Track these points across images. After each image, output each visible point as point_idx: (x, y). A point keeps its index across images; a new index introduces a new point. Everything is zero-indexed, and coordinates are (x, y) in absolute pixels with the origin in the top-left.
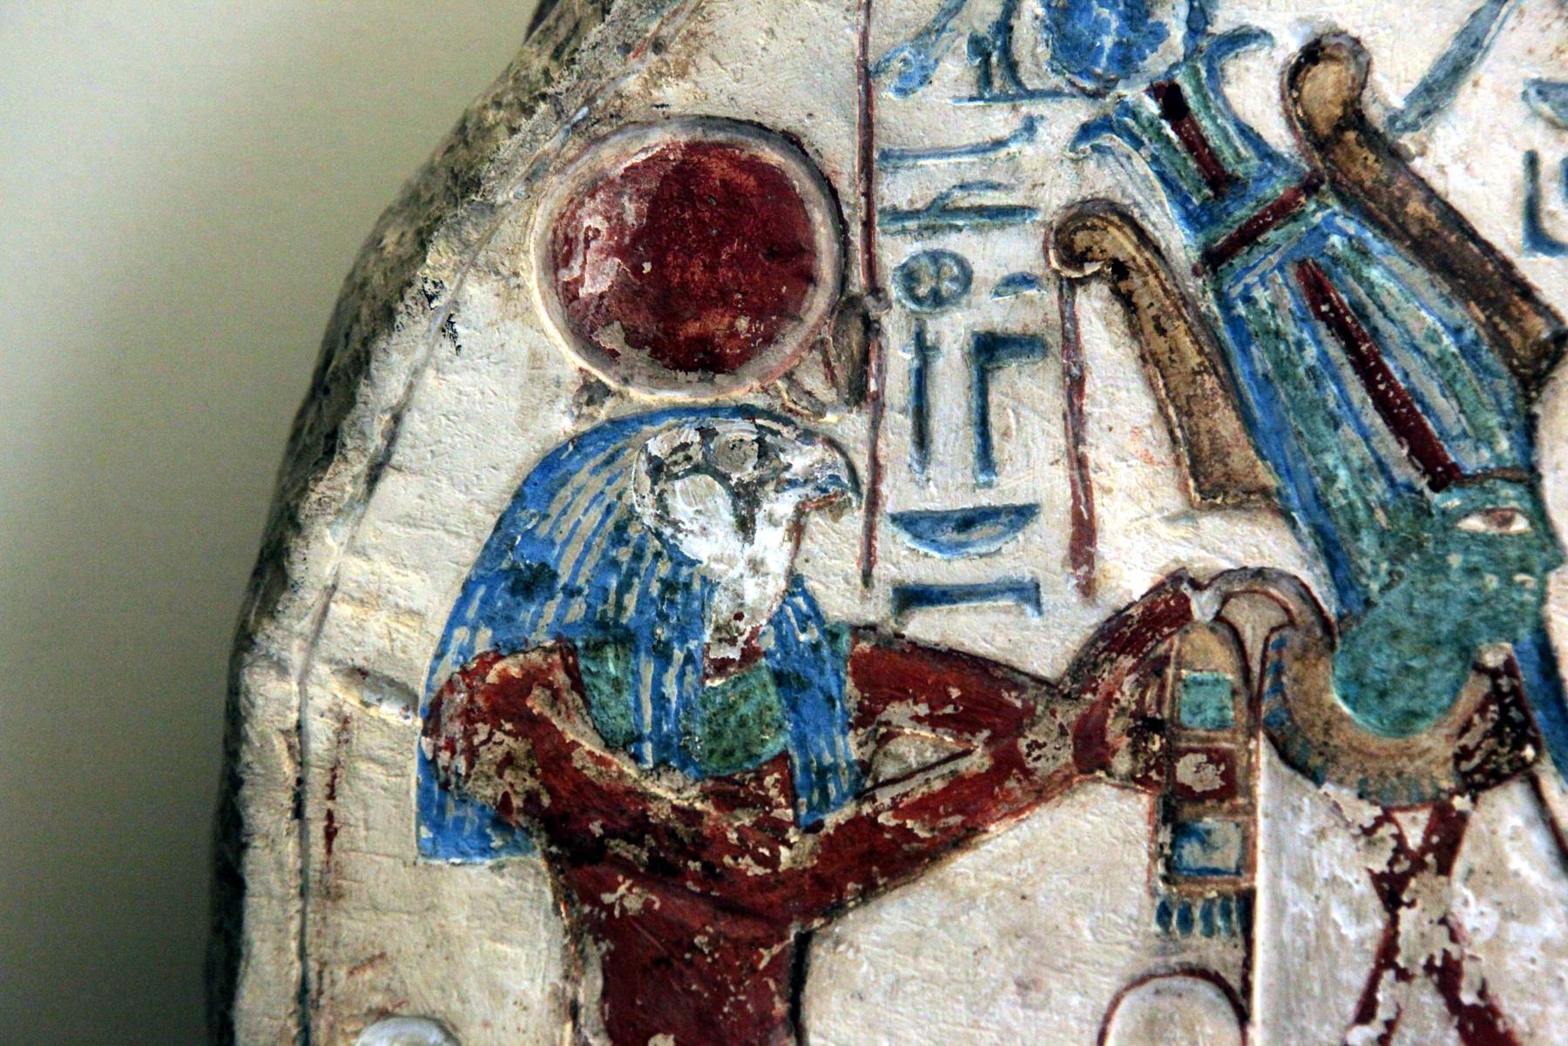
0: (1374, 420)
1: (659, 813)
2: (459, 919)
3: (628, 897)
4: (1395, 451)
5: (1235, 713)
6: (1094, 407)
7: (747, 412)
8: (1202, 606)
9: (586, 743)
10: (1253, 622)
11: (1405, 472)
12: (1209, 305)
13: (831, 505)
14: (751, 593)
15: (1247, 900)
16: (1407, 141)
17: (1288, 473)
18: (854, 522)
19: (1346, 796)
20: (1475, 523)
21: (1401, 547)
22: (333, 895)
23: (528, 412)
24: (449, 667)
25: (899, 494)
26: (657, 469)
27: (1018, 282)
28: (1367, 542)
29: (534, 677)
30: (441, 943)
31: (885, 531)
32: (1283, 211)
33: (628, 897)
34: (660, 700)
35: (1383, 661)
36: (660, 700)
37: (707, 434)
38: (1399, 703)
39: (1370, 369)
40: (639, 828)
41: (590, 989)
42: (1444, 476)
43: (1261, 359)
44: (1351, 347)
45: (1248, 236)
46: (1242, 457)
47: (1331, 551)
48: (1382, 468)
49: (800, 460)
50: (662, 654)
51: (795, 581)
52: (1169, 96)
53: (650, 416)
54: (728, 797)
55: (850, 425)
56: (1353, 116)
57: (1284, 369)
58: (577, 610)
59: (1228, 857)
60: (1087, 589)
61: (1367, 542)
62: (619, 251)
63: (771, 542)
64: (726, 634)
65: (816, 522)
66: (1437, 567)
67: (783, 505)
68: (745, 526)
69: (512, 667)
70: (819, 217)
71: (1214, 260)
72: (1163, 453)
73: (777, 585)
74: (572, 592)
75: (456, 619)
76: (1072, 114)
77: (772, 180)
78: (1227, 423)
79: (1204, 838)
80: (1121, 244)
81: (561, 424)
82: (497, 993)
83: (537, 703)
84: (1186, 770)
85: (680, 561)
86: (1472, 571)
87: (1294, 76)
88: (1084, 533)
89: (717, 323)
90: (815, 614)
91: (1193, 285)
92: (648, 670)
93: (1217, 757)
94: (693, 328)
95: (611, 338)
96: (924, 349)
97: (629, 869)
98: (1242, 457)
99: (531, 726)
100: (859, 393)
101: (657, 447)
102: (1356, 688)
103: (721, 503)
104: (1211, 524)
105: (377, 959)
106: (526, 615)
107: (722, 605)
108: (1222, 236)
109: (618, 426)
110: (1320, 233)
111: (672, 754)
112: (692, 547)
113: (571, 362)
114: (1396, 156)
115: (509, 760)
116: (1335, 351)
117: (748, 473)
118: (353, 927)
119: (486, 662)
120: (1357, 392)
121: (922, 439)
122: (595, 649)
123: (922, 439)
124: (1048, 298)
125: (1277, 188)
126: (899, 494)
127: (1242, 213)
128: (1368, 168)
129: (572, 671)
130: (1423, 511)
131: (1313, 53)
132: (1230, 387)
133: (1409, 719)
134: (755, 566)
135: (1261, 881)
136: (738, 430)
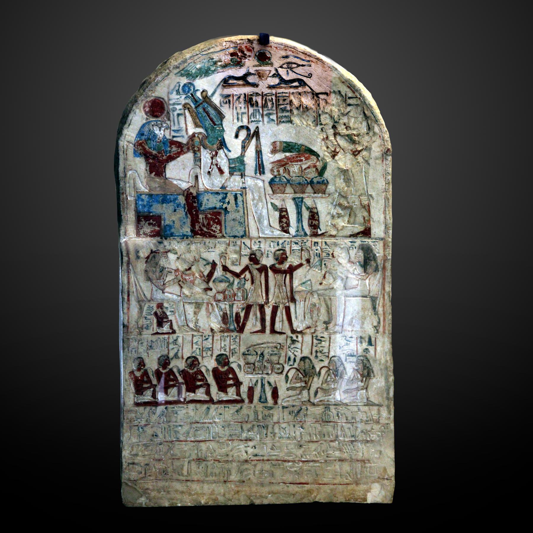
0: (209, 120)
1: (153, 154)
2: (137, 162)
3: (151, 161)
4: (211, 122)
5: (199, 144)
6: (187, 119)
7: (160, 121)
8: (196, 135)
9: (147, 147)
10: (200, 136)
11: (212, 124)
12: (196, 111)
13: (167, 129)
14: (161, 136)
15: (201, 159)
16: (211, 98)
17: (203, 124)
18: (169, 130)
19: (208, 150)
20: (218, 128)
21: (212, 130)
22: (127, 160)
23: (142, 121)
24: (136, 141)
25: (173, 128)
26: (153, 125)
27: (180, 109)
28: (209, 130)
29: (143, 142)
30: (136, 164)
31: (171, 131)
32: (201, 104)
33: (151, 161)
34: (153, 145)
35: (211, 140)
36: (153, 145)
37: (157, 123)
38: (212, 143)
39: (209, 116)
40: (152, 155)
41: (148, 168)
42: (215, 125)
43: (200, 115)
44: (207, 114)
45: (199, 105)
46: (199, 123)
47: (206, 131)
48: (210, 124)
49: (164, 125)
50: (153, 141)
51: (164, 135)
52: (192, 94)
53: (152, 121)
54: (159, 153)
55: (168, 122)
56: (206, 96)
57: (202, 116)
58: (146, 137)
59: (199, 156)
60: (187, 134)
61: (209, 130)
62: (149, 107)
63: (162, 132)
64: (159, 139)
65: (166, 130)
66: (215, 132)
67: (163, 129)
68: (160, 130)
69: (141, 141)
70: (165, 105)
71: (196, 107)
72: (193, 123)
73: (163, 135)
74: (146, 135)
75: (136, 137)
76: (183, 97)
77: (161, 102)
78: (198, 120)
79: (197, 154)
80: (189, 106)
81: (144, 121)
82: (140, 168)
83: (143, 144)
84: (196, 149)
85: (155, 133)
86: (218, 132)
87: (202, 93)
88: (187, 129)
89: (157, 114)
90: (166, 138)
91: (194, 109)
92: (152, 142)
93: (198, 147)
94: (155, 114)
95: (148, 114)
96: (173, 115)
97: (151, 159)
98: (199, 123)
99: (143, 146)
100: (169, 120)
101: (153, 124)
102: (209, 142)
103: (158, 129)
104: (197, 129)
105: (130, 165)
106: (142, 137)
107: (158, 137)
108: (197, 106)
109: (150, 122)
110: (204, 105)
111: (154, 149)
112: (156, 132)
113: (145, 116)
114: (210, 99)
115: (141, 149)
116: (206, 115)
117: (160, 126)
118: (128, 163)
119: (139, 141)
120: (208, 118)
121: (174, 124)
122: (148, 140)
123: (174, 124)
124: (183, 111)
125: (201, 102)
126: (173, 128)
127: (198, 104)
128: (208, 100)
129: (146, 142)
130: (214, 127)
131: (203, 91)
132: (198, 117)
133: (213, 144)
134: (161, 134)
135: (202, 158)
136: (159, 122)
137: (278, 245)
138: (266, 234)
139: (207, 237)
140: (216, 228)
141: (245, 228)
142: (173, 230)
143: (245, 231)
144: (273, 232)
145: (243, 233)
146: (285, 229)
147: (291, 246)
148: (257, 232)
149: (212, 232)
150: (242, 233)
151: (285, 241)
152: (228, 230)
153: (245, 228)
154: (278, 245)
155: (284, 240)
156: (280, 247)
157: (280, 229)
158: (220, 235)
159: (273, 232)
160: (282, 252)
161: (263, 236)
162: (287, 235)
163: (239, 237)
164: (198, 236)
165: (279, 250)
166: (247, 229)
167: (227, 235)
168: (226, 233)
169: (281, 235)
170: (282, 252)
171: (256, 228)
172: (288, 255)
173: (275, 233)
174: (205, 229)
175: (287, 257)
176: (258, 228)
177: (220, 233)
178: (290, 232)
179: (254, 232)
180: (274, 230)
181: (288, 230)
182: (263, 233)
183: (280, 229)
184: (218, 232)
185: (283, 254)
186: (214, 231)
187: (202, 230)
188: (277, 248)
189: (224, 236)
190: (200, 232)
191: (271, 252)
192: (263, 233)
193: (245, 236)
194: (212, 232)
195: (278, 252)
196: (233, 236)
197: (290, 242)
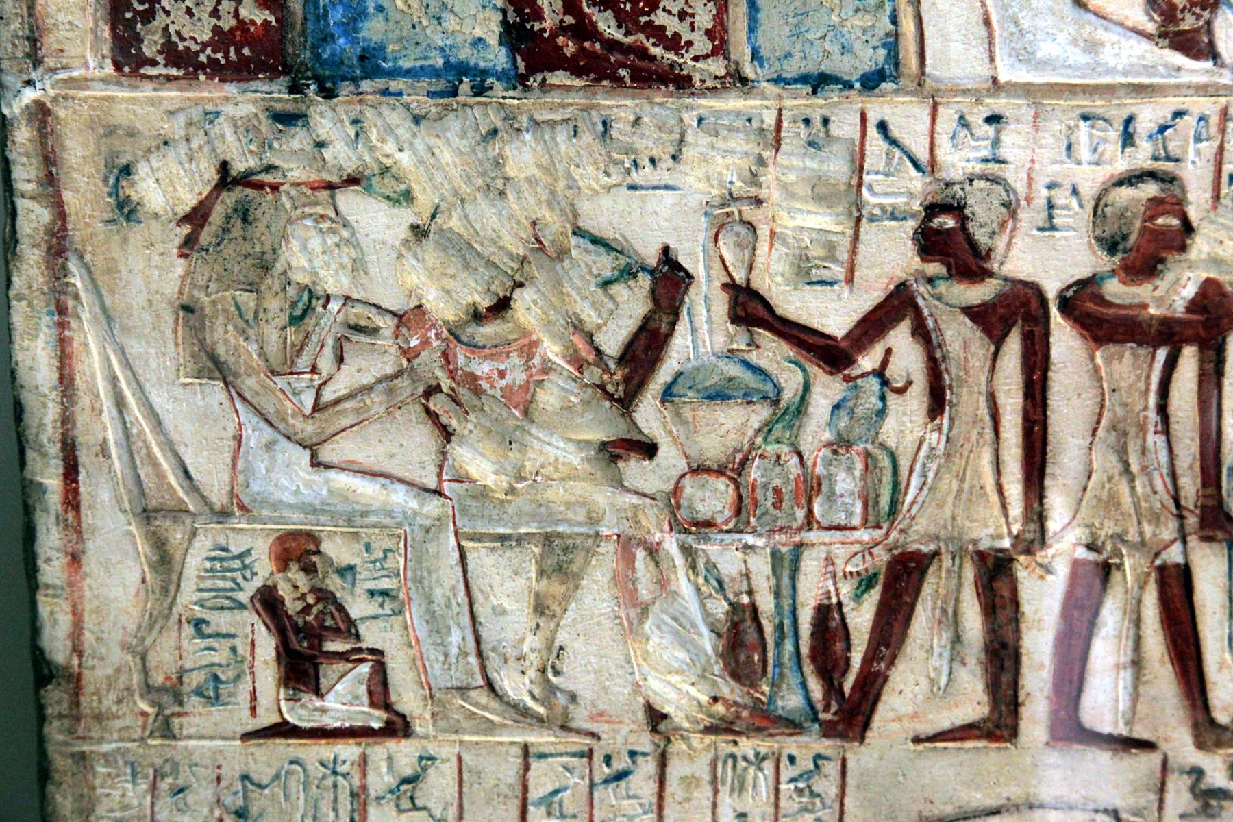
137: (1128, 139)
138: (1044, 64)
139: (618, 80)
140: (682, 15)
141: (894, 20)
142: (373, 30)
143: (892, 44)
144: (1093, 46)
145: (882, 53)
146: (1188, 23)
147: (1221, 149)
148: (980, 51)
149: (657, 51)
150: (869, 58)
151: (1178, 114)
152: (774, 34)
153: (894, 20)
154: (1128, 139)
155: (1174, 103)
156: (1142, 156)
157: (1151, 27)
158: (717, 67)
159: (1093, 46)
160: (1151, 189)
161: (1023, 75)
162: (1196, 70)
163: (849, 85)
164: (559, 77)
165: (1133, 179)
166: (908, 26)
167: (767, 71)
168: (755, 56)
169: (1151, 69)
170: (1151, 189)
171: (977, 17)
172: (1193, 214)
173: (1107, 56)
174: (606, 24)
175: (1188, 228)
176: (987, 22)
177: (715, 52)
178: (1221, 46)
179: (956, 48)
180: (1101, 34)
181: (1210, 32)
182: (1026, 57)
183: (1151, 27)
184: (702, 45)
185: (1156, 206)
186: (674, 43)
187: (583, 30)
188: (1122, 164)
189: (744, 81)
190: (570, 49)
191: (1075, 192)
192: (1026, 57)
193: (895, 79)
194: (657, 51)
195: (1126, 193)
196: (804, 79)
197: (1214, 120)
